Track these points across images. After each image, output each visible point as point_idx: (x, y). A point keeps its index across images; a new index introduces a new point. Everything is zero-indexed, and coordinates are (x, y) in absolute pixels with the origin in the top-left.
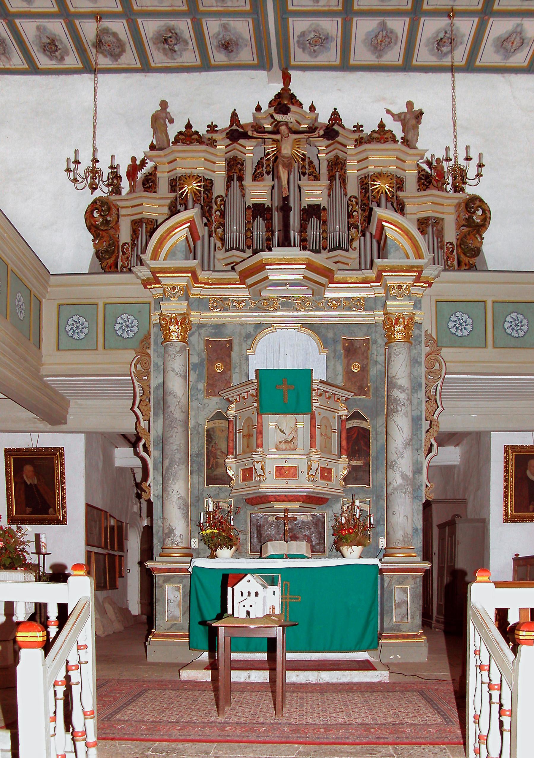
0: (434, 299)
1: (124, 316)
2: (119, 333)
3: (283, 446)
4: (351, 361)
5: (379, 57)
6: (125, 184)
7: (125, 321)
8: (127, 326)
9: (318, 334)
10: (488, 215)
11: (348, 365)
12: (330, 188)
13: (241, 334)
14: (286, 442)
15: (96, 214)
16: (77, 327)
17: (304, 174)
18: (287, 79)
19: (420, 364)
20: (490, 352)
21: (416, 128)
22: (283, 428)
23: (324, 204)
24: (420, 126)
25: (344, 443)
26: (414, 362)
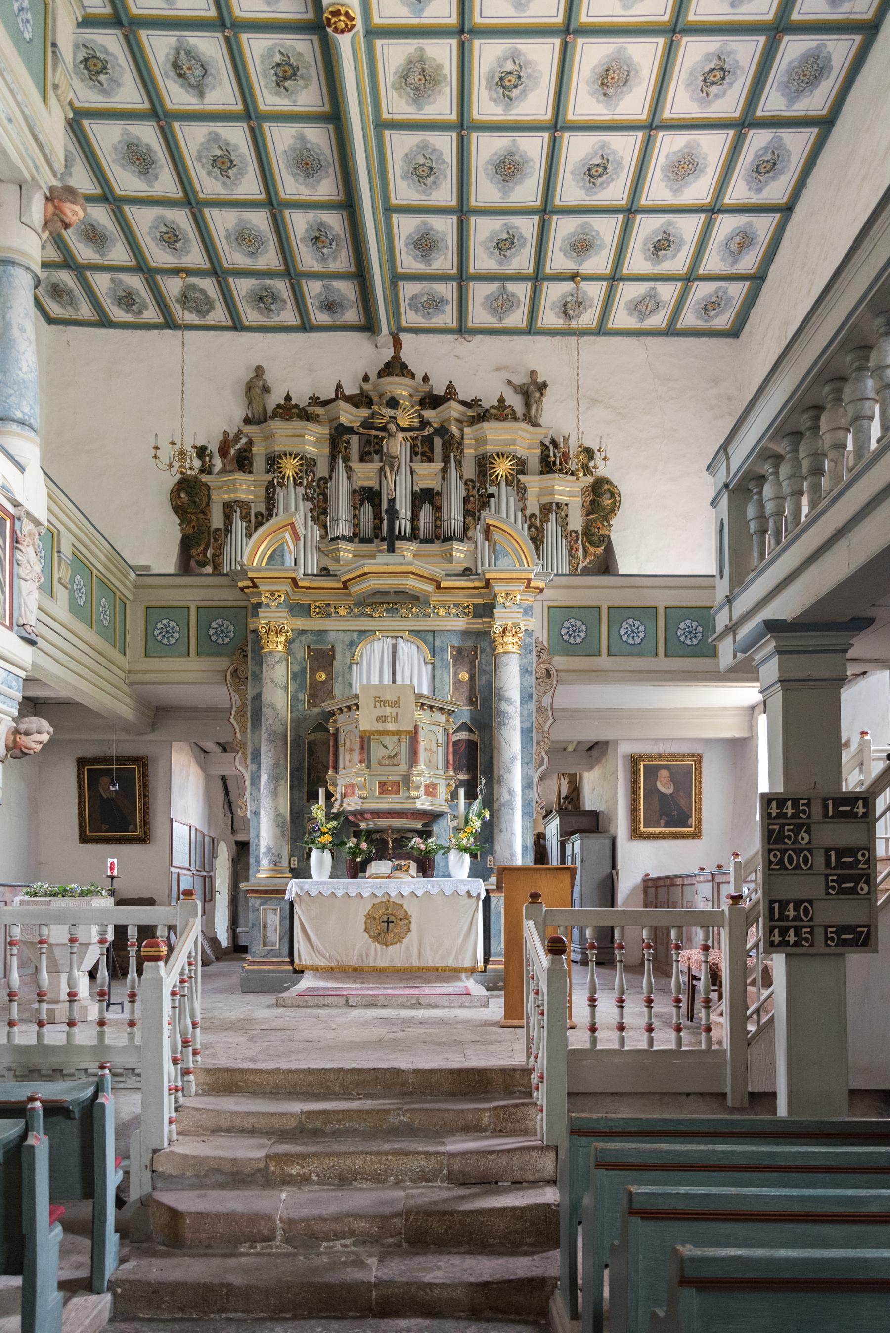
0: (546, 604)
1: (219, 621)
2: (214, 638)
3: (387, 762)
4: (459, 670)
5: (500, 319)
6: (218, 463)
7: (220, 626)
8: (222, 632)
9: (425, 642)
10: (618, 499)
11: (456, 674)
12: (444, 470)
13: (343, 642)
14: (389, 757)
15: (183, 495)
16: (167, 632)
17: (416, 454)
18: (397, 344)
19: (530, 673)
20: (604, 661)
21: (539, 402)
22: (386, 743)
23: (437, 488)
24: (544, 399)
25: (451, 757)
26: (525, 671)
